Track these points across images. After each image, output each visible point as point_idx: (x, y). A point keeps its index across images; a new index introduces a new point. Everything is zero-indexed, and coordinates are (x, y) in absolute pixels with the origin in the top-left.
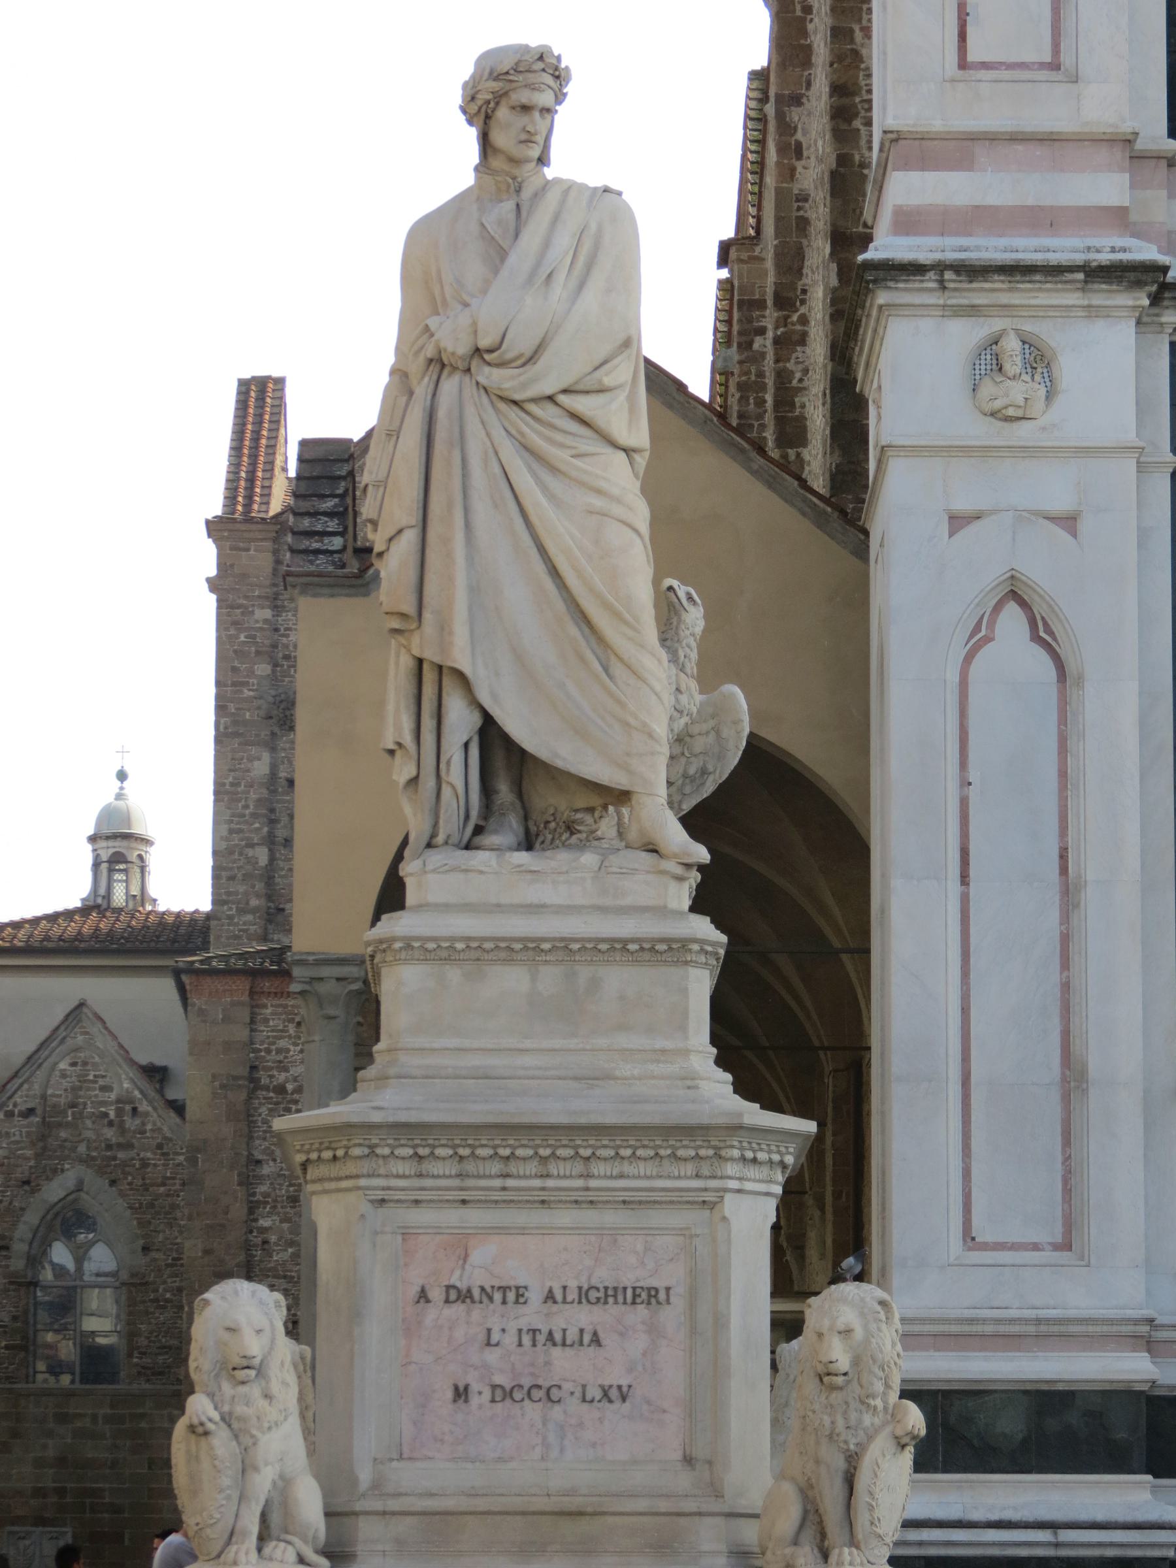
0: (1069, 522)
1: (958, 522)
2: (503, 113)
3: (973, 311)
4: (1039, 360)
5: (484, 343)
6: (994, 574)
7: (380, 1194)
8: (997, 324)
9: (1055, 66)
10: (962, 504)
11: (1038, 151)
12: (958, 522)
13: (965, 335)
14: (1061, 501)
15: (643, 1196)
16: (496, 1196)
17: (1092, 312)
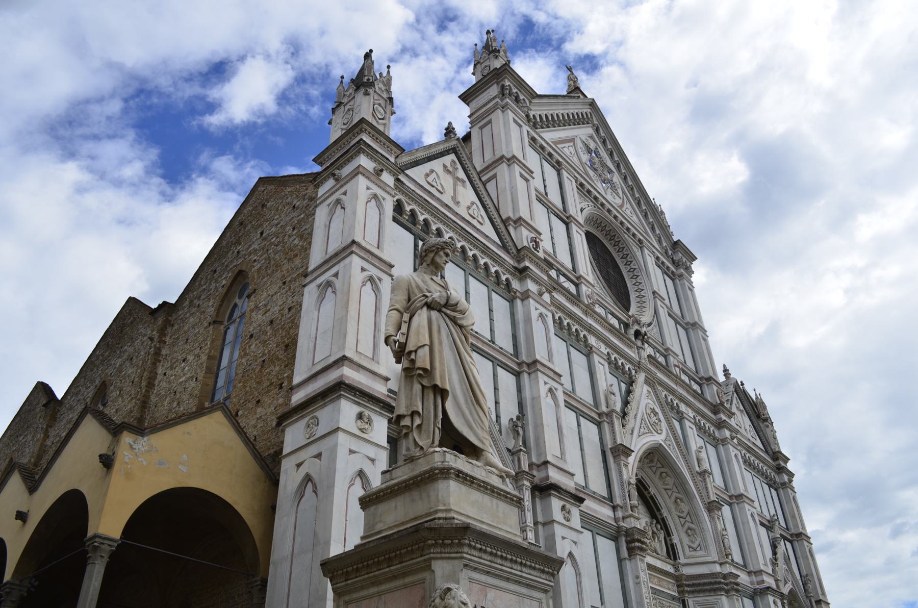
0: (373, 460)
1: (351, 452)
2: (442, 253)
3: (358, 404)
4: (370, 422)
5: (452, 302)
6: (358, 468)
7: (467, 562)
8: (363, 409)
9: (373, 359)
10: (353, 448)
11: (372, 375)
12: (351, 452)
13: (356, 409)
14: (372, 456)
15: (532, 583)
16: (498, 572)
17: (381, 415)
